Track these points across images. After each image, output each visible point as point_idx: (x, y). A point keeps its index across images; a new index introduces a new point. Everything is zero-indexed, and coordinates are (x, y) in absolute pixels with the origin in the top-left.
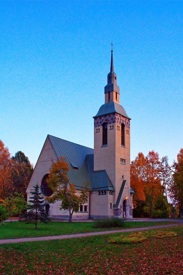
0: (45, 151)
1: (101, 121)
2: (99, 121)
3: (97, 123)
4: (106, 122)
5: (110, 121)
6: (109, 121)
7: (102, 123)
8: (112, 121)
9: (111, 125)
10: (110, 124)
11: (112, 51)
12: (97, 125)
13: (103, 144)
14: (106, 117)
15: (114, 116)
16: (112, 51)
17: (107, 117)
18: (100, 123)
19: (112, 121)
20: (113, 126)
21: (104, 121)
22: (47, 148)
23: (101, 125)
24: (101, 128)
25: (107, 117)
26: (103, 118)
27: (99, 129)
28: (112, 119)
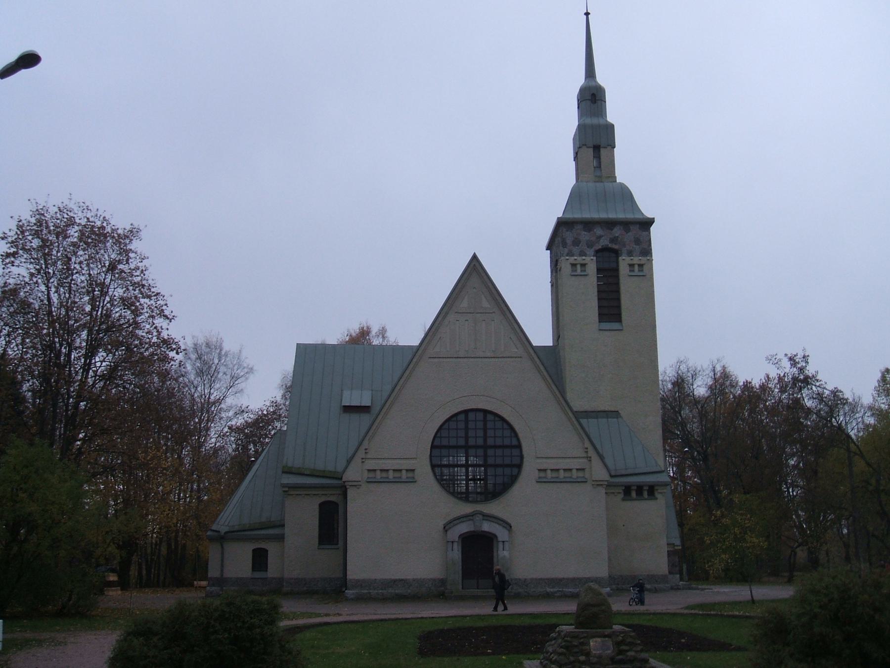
0: (451, 317)
1: (593, 239)
2: (585, 236)
3: (576, 242)
4: (615, 247)
6: (624, 245)
9: (636, 260)
10: (630, 253)
11: (587, 14)
12: (576, 250)
14: (612, 230)
15: (645, 233)
16: (587, 14)
17: (615, 230)
18: (590, 245)
20: (641, 266)
21: (604, 242)
22: (464, 304)
23: (591, 252)
25: (617, 231)
27: (583, 265)
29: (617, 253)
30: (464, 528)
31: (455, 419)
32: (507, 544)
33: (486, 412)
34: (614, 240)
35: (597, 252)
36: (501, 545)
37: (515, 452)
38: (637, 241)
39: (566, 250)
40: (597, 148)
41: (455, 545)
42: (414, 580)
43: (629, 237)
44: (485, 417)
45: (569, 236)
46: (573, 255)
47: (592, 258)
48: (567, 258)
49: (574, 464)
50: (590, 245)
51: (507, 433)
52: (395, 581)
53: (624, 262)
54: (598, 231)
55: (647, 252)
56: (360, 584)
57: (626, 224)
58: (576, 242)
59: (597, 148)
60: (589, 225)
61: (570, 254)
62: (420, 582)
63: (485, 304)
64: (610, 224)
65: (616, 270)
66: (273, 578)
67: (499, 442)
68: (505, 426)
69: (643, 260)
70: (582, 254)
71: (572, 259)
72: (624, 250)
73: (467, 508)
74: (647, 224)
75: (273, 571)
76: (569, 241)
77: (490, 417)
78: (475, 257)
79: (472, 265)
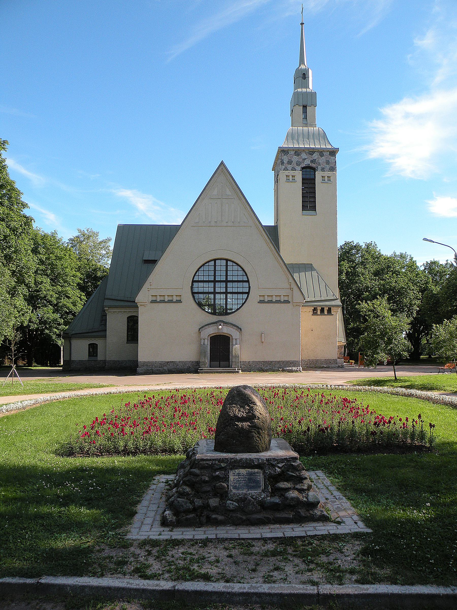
1: (301, 160)
2: (295, 159)
3: (290, 162)
4: (313, 165)
5: (322, 166)
7: (303, 165)
8: (328, 167)
9: (326, 174)
10: (323, 170)
11: (302, 24)
12: (289, 167)
13: (304, 208)
16: (302, 24)
19: (328, 167)
21: (307, 162)
23: (299, 168)
24: (299, 175)
25: (315, 156)
26: (304, 155)
28: (328, 162)
29: (314, 170)
30: (212, 331)
31: (208, 264)
32: (238, 341)
33: (227, 260)
34: (313, 161)
35: (303, 168)
36: (234, 341)
37: (246, 285)
38: (328, 162)
39: (283, 167)
40: (305, 107)
41: (206, 341)
42: (180, 362)
43: (322, 160)
44: (227, 263)
45: (286, 159)
46: (287, 170)
47: (300, 172)
48: (284, 171)
49: (283, 293)
50: (298, 164)
51: (241, 273)
52: (168, 362)
53: (319, 175)
54: (304, 155)
55: (333, 169)
56: (145, 364)
57: (321, 152)
58: (290, 162)
59: (305, 107)
60: (298, 152)
61: (286, 169)
62: (184, 363)
63: (228, 192)
64: (311, 152)
65: (314, 179)
66: (101, 361)
67: (235, 279)
68: (240, 269)
69: (330, 174)
70: (293, 169)
71: (287, 173)
72: (319, 168)
73: (215, 318)
74: (333, 152)
75: (100, 357)
76: (285, 161)
77: (229, 263)
78: (222, 163)
79: (220, 168)
